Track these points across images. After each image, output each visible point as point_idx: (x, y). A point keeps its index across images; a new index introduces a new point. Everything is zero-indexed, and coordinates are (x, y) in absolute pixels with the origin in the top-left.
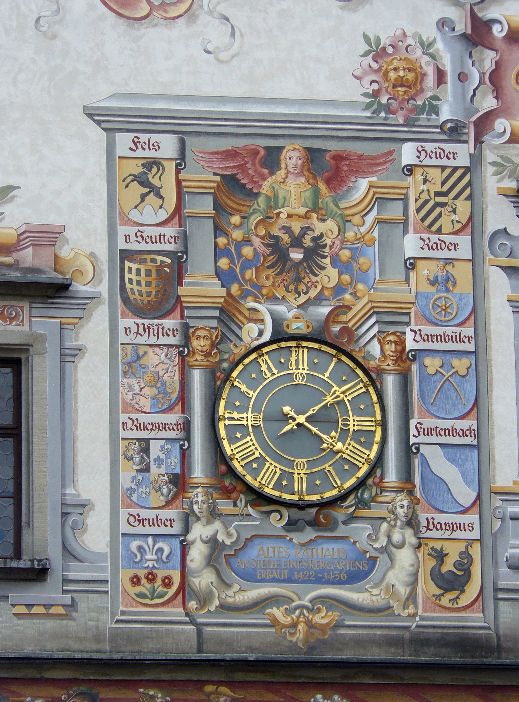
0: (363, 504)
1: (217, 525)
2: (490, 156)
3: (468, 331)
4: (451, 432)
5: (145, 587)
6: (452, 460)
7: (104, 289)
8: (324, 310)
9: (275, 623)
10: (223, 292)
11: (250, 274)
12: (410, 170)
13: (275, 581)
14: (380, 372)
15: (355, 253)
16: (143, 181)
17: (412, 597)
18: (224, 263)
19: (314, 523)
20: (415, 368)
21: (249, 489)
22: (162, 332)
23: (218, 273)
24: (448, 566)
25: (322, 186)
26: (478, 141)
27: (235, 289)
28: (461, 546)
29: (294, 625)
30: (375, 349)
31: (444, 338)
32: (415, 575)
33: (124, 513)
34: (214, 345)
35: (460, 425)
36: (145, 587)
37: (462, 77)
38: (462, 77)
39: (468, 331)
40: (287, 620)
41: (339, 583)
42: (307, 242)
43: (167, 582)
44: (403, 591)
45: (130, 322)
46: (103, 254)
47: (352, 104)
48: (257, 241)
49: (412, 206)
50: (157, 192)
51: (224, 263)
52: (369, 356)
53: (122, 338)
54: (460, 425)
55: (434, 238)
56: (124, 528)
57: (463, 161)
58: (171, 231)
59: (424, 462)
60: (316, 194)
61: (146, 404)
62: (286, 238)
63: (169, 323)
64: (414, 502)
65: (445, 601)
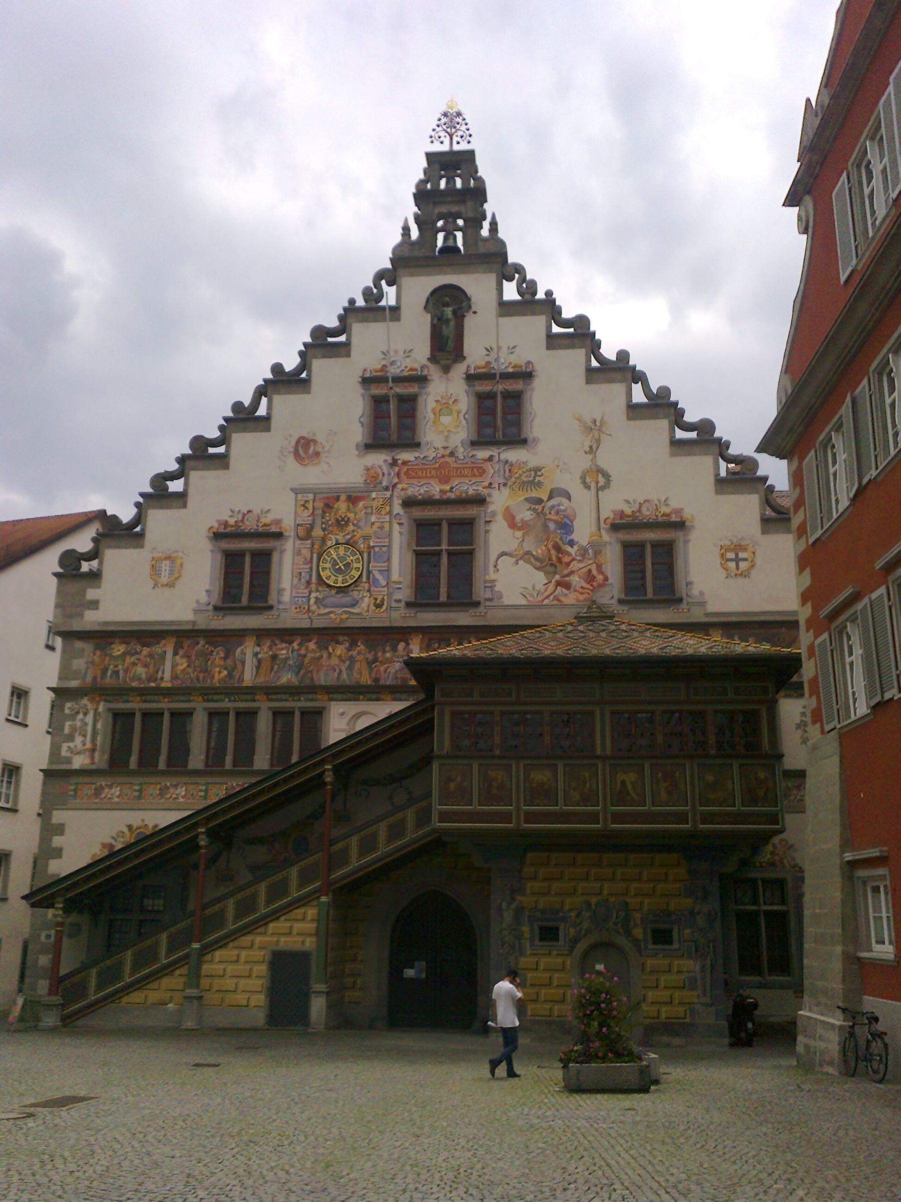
0: (357, 586)
1: (318, 593)
2: (395, 494)
3: (387, 540)
4: (381, 567)
5: (298, 610)
6: (381, 574)
7: (292, 534)
8: (349, 537)
9: (331, 618)
10: (323, 533)
11: (330, 528)
12: (374, 499)
13: (332, 607)
14: (363, 552)
15: (358, 521)
16: (303, 506)
17: (368, 611)
18: (324, 526)
19: (343, 592)
20: (372, 551)
21: (326, 584)
22: (306, 544)
23: (322, 528)
24: (378, 602)
25: (351, 505)
26: (393, 491)
27: (326, 532)
28: (382, 596)
29: (336, 619)
30: (362, 546)
31: (380, 542)
32: (369, 604)
33: (294, 591)
34: (320, 547)
35: (383, 565)
36: (298, 609)
37: (389, 474)
38: (389, 474)
39: (387, 540)
40: (334, 617)
41: (347, 607)
42: (346, 519)
43: (304, 608)
44: (366, 609)
45: (299, 542)
46: (292, 524)
47: (360, 483)
48: (333, 520)
49: (374, 509)
50: (307, 508)
51: (324, 526)
52: (360, 548)
53: (296, 546)
54: (383, 565)
55: (379, 516)
56: (294, 595)
57: (389, 496)
58: (310, 518)
59: (373, 575)
60: (349, 506)
61: (301, 563)
62: (340, 519)
63: (309, 542)
64: (370, 586)
65: (377, 611)
